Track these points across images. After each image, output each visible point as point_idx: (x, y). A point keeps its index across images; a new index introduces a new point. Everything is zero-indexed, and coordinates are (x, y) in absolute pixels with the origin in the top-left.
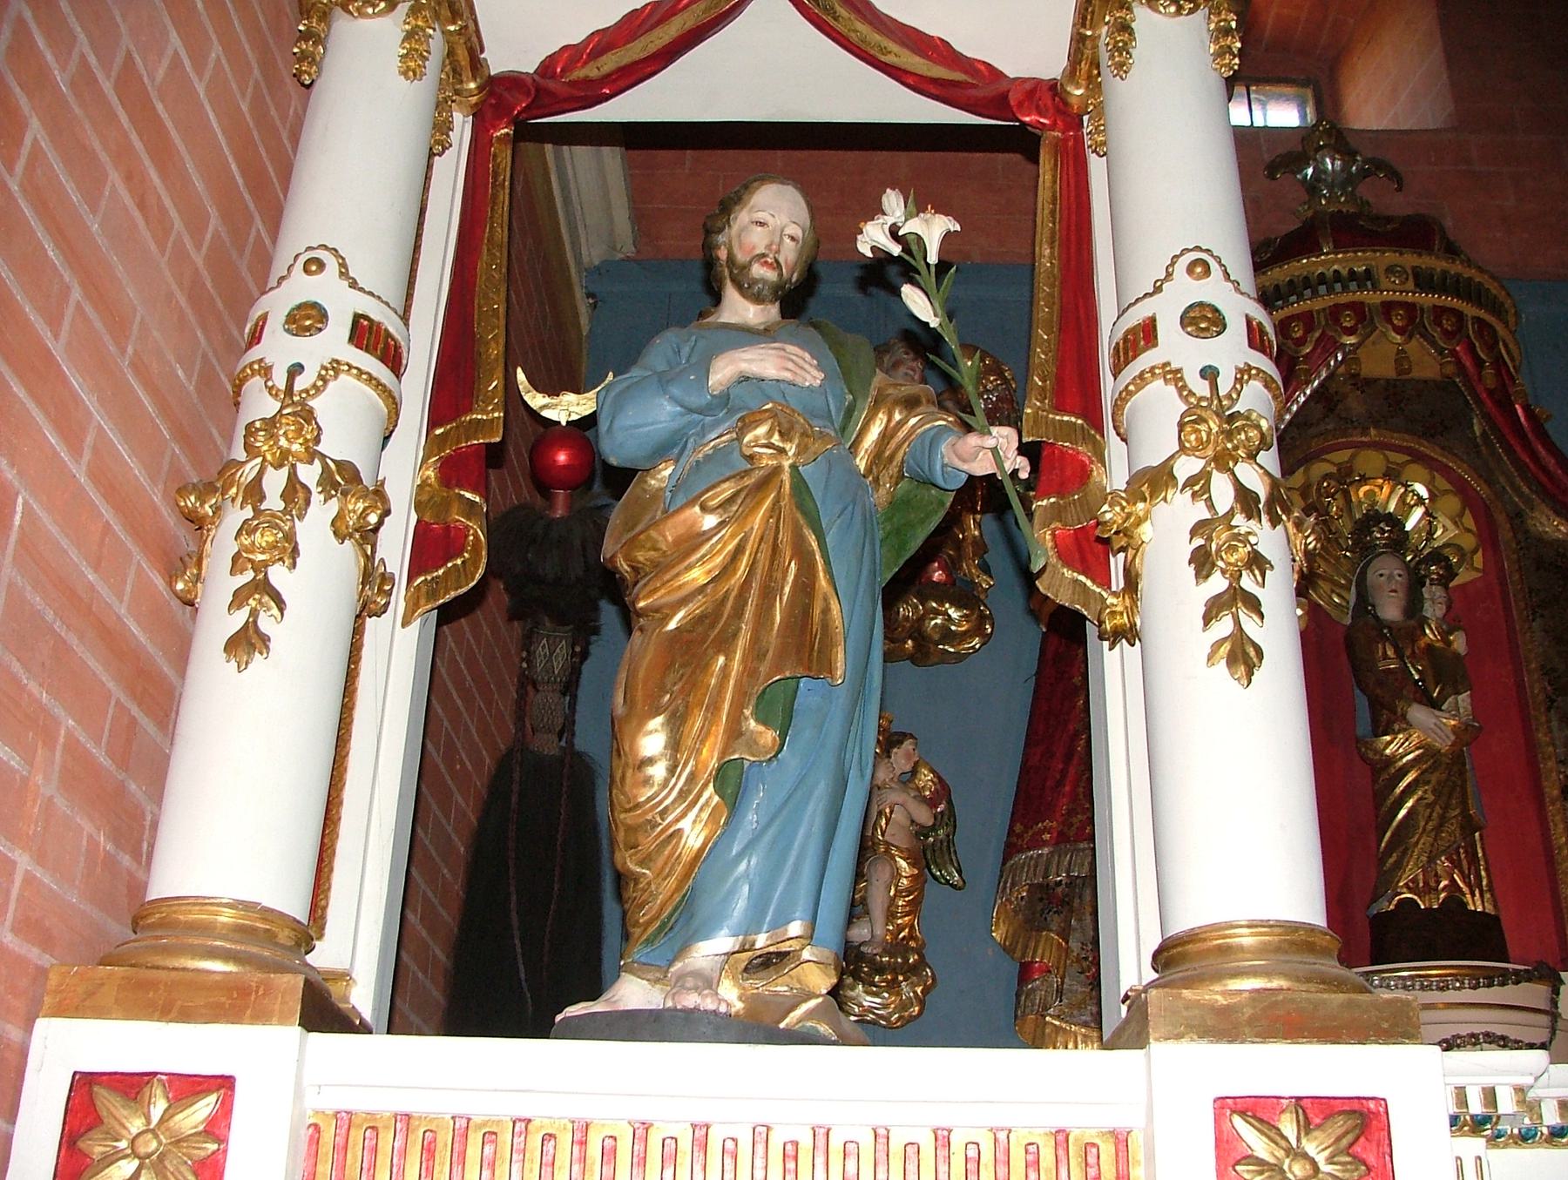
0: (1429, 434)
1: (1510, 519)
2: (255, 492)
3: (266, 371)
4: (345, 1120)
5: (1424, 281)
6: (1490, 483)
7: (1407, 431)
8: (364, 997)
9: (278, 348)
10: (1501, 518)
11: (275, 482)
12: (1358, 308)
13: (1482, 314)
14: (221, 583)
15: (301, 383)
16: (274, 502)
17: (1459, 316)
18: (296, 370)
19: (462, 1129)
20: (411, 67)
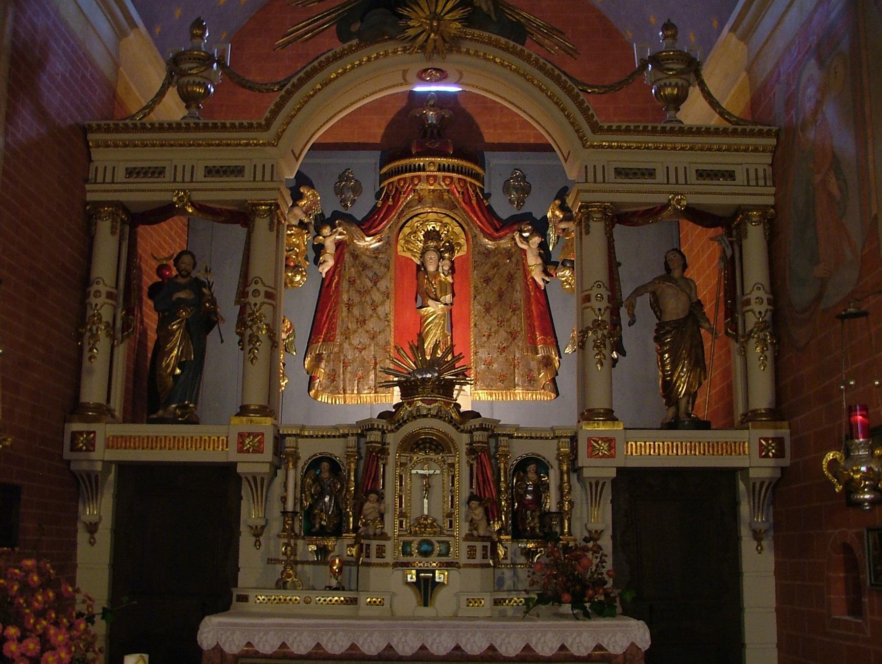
0: (451, 209)
1: (472, 238)
2: (91, 330)
3: (91, 305)
4: (113, 437)
5: (442, 168)
6: (468, 225)
7: (445, 208)
8: (118, 413)
9: (93, 300)
10: (470, 237)
11: (94, 328)
12: (419, 177)
13: (460, 176)
14: (87, 348)
15: (98, 307)
16: (95, 331)
17: (451, 178)
18: (96, 305)
19: (130, 437)
20: (113, 233)
